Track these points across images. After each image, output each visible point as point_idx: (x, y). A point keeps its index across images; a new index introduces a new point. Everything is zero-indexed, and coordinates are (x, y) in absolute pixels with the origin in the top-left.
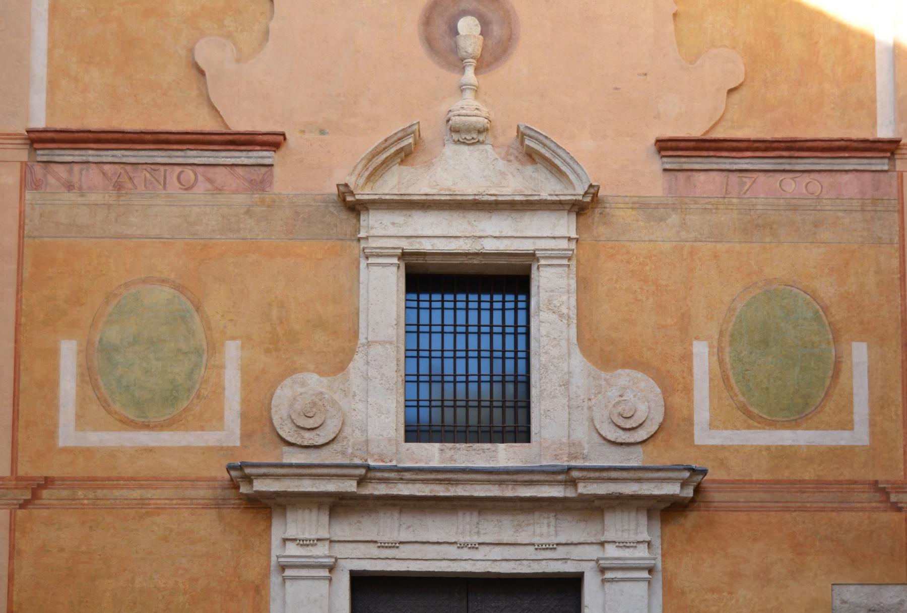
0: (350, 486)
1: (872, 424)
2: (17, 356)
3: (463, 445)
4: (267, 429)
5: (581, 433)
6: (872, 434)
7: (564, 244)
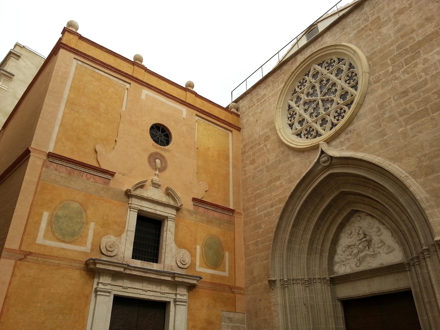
0: (122, 270)
1: (229, 272)
2: (30, 213)
3: (146, 262)
4: (98, 249)
5: (174, 264)
6: (229, 274)
7: (174, 216)
